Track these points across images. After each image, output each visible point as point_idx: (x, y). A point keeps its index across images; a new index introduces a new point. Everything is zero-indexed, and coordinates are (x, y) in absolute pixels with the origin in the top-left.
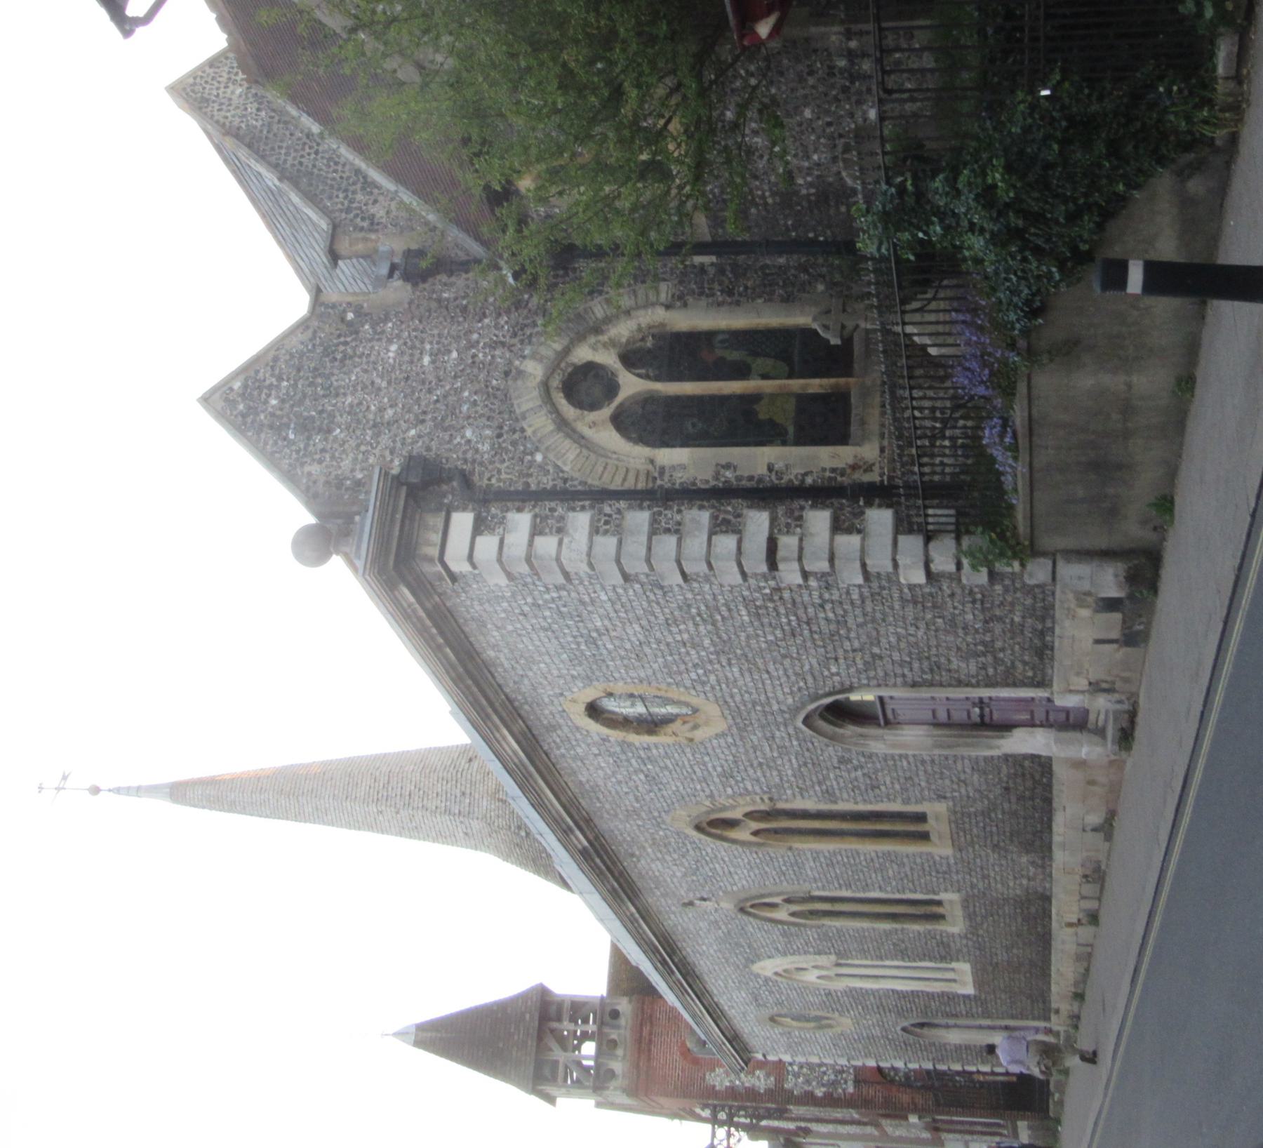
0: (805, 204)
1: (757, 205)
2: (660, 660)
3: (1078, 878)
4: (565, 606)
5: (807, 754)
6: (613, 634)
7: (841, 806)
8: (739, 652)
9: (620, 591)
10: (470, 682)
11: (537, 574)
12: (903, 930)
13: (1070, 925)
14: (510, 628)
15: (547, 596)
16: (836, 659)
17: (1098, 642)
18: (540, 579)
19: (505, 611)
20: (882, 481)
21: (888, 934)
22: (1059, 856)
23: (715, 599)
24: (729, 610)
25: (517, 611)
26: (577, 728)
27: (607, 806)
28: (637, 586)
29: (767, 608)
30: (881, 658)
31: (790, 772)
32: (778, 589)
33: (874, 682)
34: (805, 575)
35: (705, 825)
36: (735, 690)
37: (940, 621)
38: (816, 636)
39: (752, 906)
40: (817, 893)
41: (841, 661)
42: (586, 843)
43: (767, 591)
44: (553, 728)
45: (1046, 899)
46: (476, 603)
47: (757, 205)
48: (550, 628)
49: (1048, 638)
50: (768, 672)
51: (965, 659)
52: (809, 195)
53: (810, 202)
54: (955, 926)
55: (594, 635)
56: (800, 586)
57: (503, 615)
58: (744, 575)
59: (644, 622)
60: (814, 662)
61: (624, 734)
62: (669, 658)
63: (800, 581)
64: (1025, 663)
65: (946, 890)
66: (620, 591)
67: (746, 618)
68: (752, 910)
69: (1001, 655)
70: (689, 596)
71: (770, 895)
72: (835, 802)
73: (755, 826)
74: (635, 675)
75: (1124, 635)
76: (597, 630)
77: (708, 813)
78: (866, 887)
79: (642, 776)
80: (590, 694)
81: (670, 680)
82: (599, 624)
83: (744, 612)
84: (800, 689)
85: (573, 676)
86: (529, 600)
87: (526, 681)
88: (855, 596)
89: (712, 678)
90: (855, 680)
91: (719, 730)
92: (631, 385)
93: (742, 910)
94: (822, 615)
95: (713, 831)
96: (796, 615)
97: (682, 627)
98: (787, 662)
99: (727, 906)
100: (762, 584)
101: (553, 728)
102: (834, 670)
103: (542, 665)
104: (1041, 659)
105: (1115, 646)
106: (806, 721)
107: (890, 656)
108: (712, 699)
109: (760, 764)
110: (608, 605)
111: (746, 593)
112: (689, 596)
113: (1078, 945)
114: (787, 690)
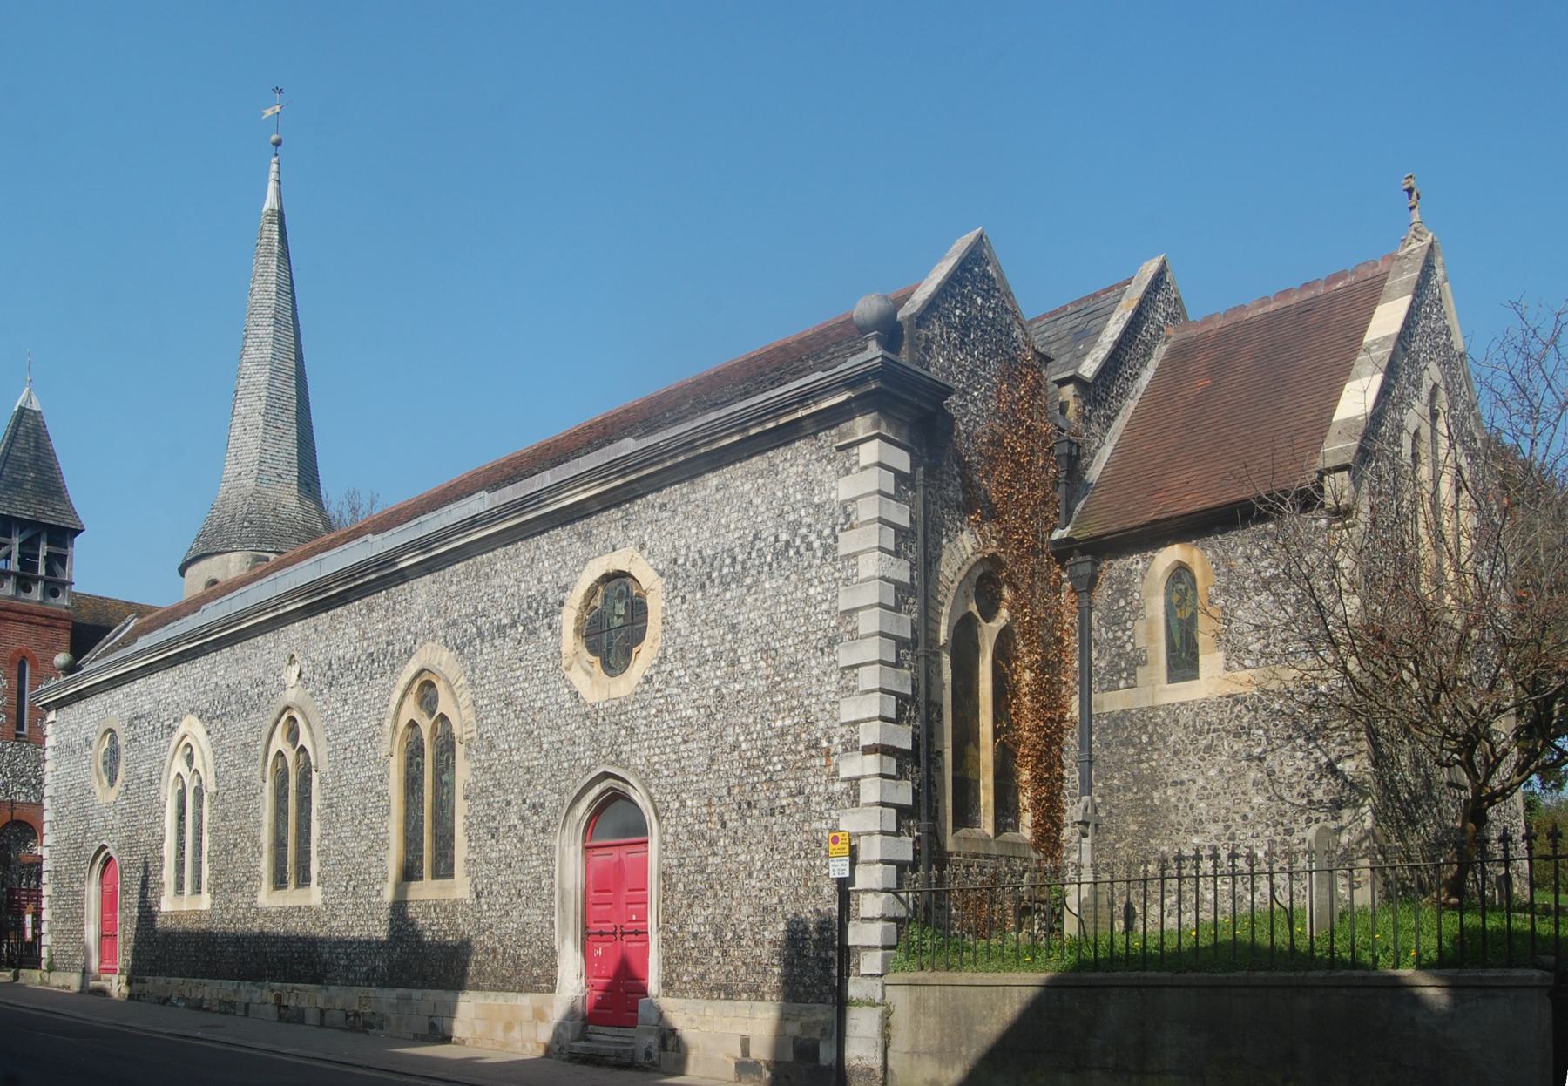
0: (1141, 795)
1: (1139, 754)
2: (706, 643)
3: (356, 1008)
4: (797, 553)
5: (546, 775)
6: (749, 600)
7: (461, 808)
8: (718, 717)
9: (825, 606)
10: (681, 458)
11: (852, 527)
12: (261, 854)
13: (278, 998)
14: (757, 501)
15: (813, 537)
16: (709, 805)
17: (745, 1043)
18: (842, 530)
19: (786, 496)
20: (951, 854)
21: (255, 840)
22: (390, 995)
23: (809, 695)
24: (792, 709)
25: (786, 508)
26: (586, 561)
27: (453, 588)
28: (833, 623)
29: (797, 743)
30: (711, 844)
31: (516, 758)
32: (828, 754)
33: (669, 838)
34: (854, 781)
35: (425, 677)
36: (653, 711)
37: (775, 900)
38: (748, 788)
39: (292, 719)
40: (315, 777)
41: (705, 810)
42: (401, 566)
43: (824, 744)
44: (586, 537)
45: (317, 979)
46: (801, 469)
47: (1139, 754)
48: (755, 537)
49: (744, 996)
50: (685, 742)
51: (711, 921)
52: (1152, 799)
53: (1142, 799)
54: (267, 898)
55: (748, 581)
56: (836, 773)
57: (780, 494)
58: (856, 723)
59: (771, 628)
60: (702, 785)
61: (577, 606)
62: (709, 651)
63: (843, 774)
64: (702, 976)
65: (326, 893)
66: (825, 606)
67: (779, 723)
68: (286, 716)
69: (716, 953)
70: (815, 672)
71: (312, 735)
72: (466, 798)
73: (426, 725)
74: (679, 617)
75: (756, 1062)
76: (756, 583)
77: (447, 681)
78: (326, 822)
79: (506, 621)
80: (645, 574)
81: (670, 651)
82: (767, 585)
83: (788, 722)
84: (657, 771)
85: (675, 561)
86: (808, 520)
87: (665, 514)
88: (816, 825)
89: (675, 691)
90: (673, 822)
91: (582, 693)
92: (988, 633)
93: (287, 708)
94: (783, 793)
95: (416, 685)
96: (784, 769)
97: (762, 663)
98: (704, 760)
99: (291, 696)
100: (836, 740)
101: (586, 537)
102: (689, 803)
103: (694, 530)
104: (710, 989)
105: (739, 1054)
106: (606, 775)
107: (715, 854)
108: (639, 690)
109: (530, 733)
110: (799, 595)
111: (821, 724)
112: (815, 672)
113: (247, 1005)
114: (656, 759)
